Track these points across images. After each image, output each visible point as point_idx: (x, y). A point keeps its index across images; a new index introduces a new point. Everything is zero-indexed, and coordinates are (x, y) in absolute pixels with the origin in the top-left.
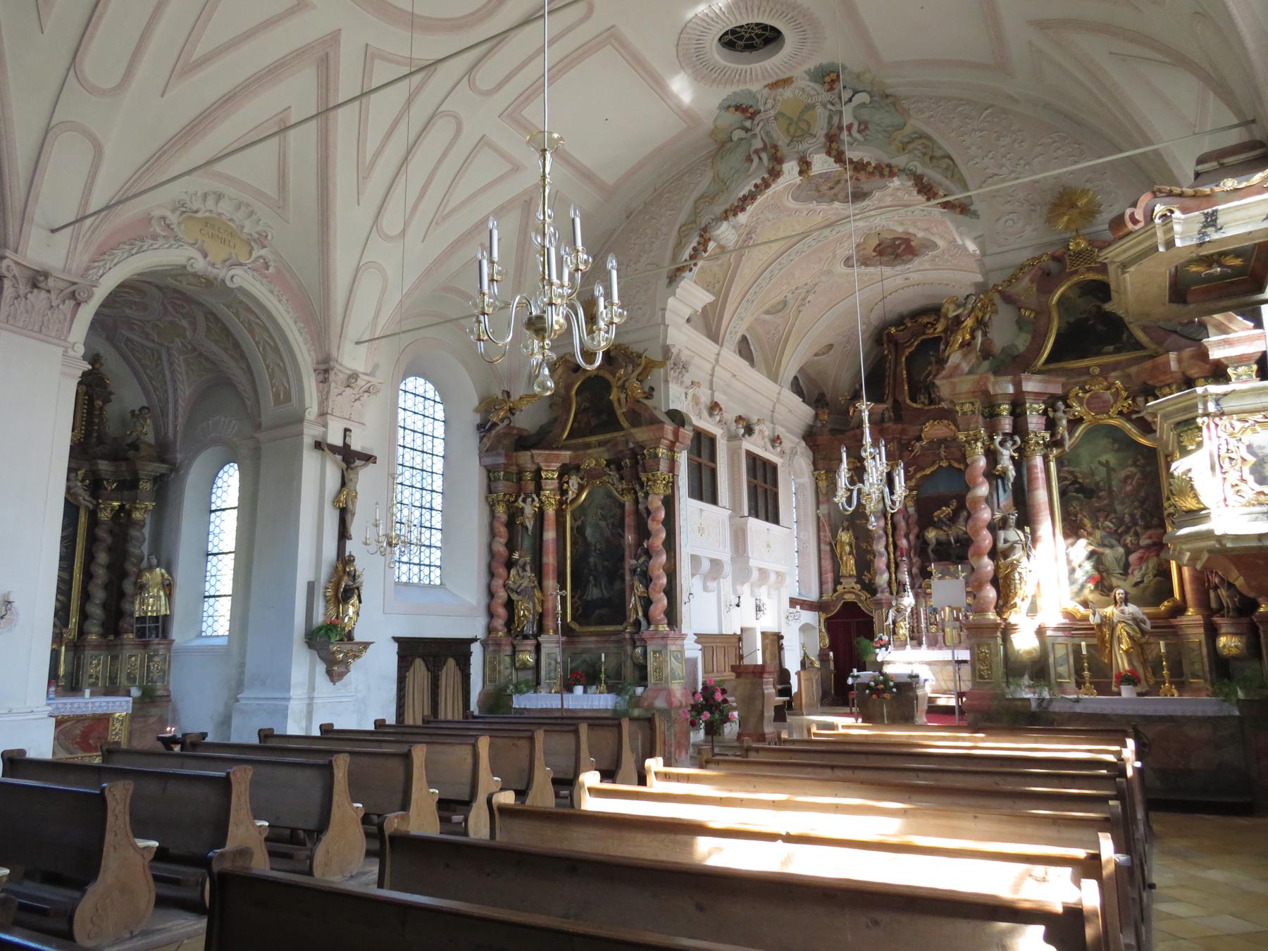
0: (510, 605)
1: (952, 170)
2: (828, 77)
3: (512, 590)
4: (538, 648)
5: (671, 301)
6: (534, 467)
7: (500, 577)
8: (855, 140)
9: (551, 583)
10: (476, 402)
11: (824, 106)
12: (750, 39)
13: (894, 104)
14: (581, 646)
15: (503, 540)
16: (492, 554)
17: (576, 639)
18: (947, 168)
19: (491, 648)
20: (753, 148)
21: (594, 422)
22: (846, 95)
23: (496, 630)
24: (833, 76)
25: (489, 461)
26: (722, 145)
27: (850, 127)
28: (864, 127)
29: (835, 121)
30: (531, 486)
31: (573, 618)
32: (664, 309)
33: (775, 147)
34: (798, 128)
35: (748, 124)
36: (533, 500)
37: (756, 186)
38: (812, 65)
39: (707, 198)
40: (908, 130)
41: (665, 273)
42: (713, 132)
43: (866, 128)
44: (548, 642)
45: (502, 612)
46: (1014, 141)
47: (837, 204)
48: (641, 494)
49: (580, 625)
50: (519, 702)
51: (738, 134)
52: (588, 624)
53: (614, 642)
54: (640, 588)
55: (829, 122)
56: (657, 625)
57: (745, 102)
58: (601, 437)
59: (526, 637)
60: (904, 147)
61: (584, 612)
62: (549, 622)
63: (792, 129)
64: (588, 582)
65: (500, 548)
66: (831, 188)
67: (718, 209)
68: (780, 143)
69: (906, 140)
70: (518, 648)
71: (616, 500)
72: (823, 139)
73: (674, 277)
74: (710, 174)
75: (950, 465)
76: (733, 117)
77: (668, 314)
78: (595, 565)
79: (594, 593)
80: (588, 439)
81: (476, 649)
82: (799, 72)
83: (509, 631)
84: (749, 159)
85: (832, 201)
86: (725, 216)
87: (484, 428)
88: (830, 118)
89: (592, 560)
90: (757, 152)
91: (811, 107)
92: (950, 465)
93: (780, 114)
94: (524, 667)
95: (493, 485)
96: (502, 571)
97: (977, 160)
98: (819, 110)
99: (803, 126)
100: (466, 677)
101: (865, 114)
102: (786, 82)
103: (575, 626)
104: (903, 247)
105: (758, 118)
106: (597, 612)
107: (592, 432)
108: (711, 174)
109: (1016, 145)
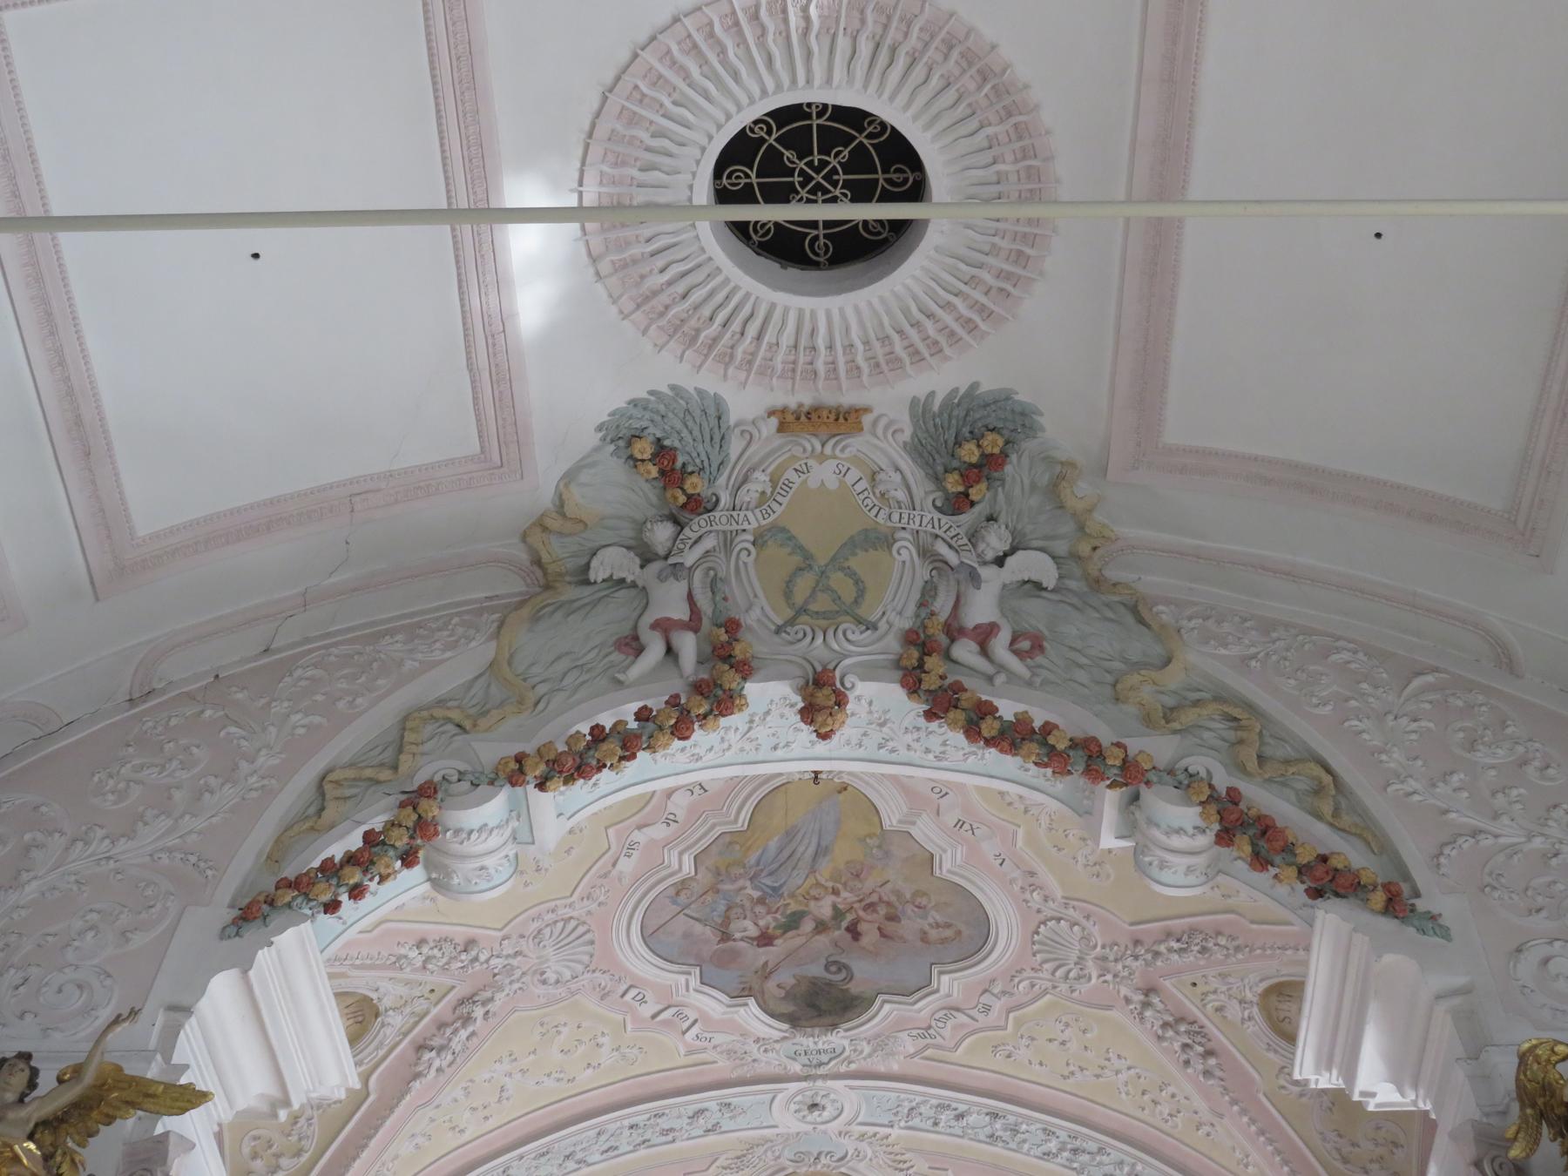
1: (1328, 791)
2: (972, 451)
5: (222, 988)
8: (1001, 668)
11: (926, 553)
12: (820, 184)
13: (1134, 610)
18: (1319, 791)
20: (648, 619)
22: (996, 541)
24: (993, 444)
26: (552, 572)
27: (984, 636)
28: (1030, 645)
29: (943, 605)
32: (181, 1010)
33: (732, 626)
34: (823, 588)
35: (662, 534)
37: (643, 715)
38: (941, 379)
39: (456, 716)
40: (1173, 679)
41: (241, 868)
42: (541, 525)
43: (1038, 646)
46: (1524, 762)
47: (751, 1016)
51: (613, 562)
55: (922, 604)
57: (688, 451)
60: (1165, 718)
63: (804, 585)
66: (765, 939)
67: (491, 750)
68: (750, 619)
69: (1170, 701)
72: (893, 644)
73: (255, 913)
74: (480, 652)
76: (620, 493)
77: (191, 1029)
82: (891, 400)
84: (633, 645)
85: (742, 992)
86: (515, 772)
88: (928, 593)
90: (665, 627)
91: (885, 541)
93: (777, 530)
97: (1412, 784)
98: (905, 551)
99: (847, 591)
101: (1036, 612)
102: (845, 420)
105: (698, 524)
108: (490, 650)
109: (1530, 770)
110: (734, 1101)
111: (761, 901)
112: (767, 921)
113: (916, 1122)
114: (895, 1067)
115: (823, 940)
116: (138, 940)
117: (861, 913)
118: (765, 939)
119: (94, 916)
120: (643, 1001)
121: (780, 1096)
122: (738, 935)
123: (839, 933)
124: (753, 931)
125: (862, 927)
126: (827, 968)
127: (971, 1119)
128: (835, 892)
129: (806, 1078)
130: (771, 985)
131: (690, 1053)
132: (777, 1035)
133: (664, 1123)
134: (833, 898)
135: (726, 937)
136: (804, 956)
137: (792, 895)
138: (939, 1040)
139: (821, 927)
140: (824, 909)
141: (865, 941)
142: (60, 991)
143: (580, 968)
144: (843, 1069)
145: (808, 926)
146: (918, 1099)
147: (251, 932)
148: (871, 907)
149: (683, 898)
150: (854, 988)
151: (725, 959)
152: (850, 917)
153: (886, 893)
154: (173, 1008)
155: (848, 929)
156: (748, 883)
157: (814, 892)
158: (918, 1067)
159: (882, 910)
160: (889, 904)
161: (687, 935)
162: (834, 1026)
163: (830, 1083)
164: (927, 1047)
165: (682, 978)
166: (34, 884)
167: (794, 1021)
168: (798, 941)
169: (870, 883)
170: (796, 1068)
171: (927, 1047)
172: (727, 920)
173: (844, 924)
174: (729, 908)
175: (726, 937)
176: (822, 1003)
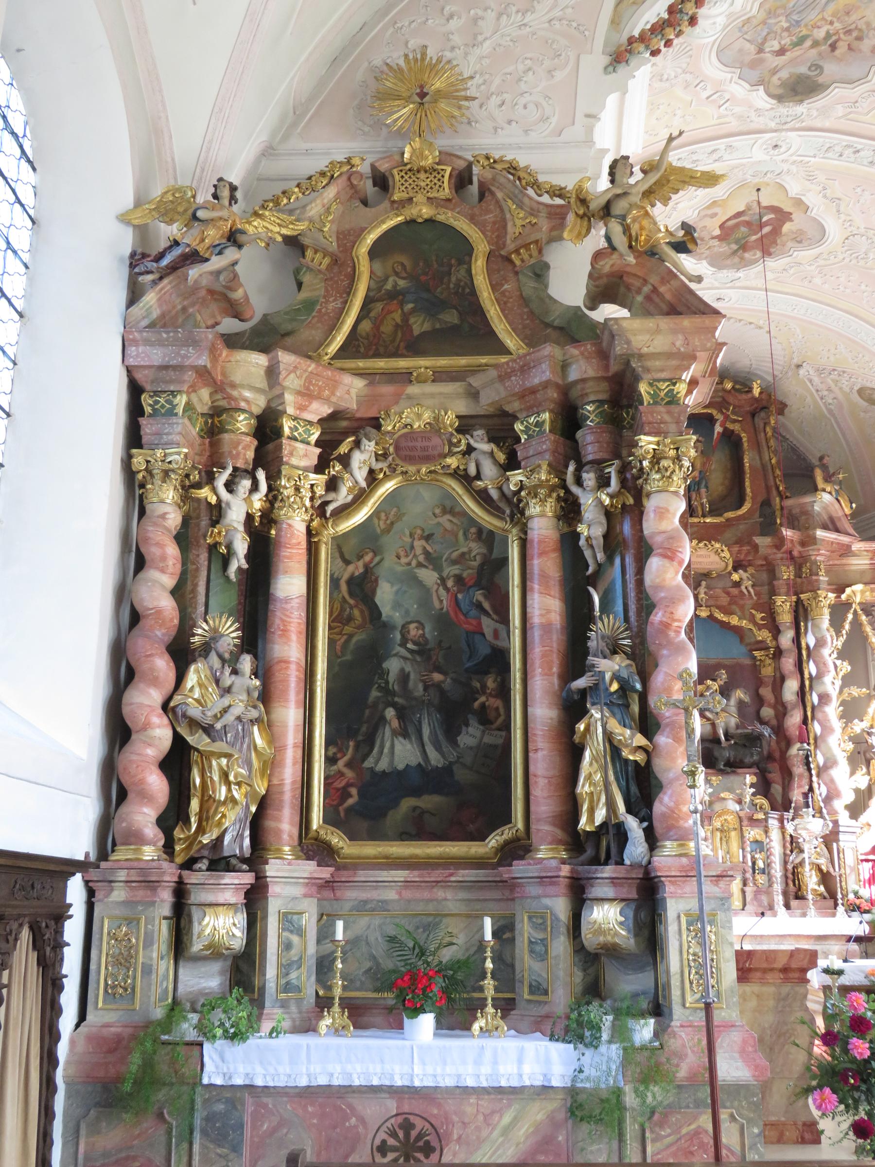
0: (177, 761)
3: (194, 724)
4: (255, 899)
6: (258, 403)
7: (155, 682)
9: (290, 715)
10: (128, 201)
14: (352, 895)
15: (169, 581)
16: (130, 617)
17: (344, 875)
19: (119, 894)
21: (419, 325)
23: (136, 838)
25: (150, 355)
30: (245, 450)
31: (330, 819)
36: (255, 487)
44: (288, 880)
45: (157, 784)
48: (592, 502)
49: (353, 837)
50: (226, 1064)
52: (375, 835)
53: (462, 885)
54: (631, 739)
56: (683, 837)
58: (443, 362)
59: (220, 863)
61: (368, 804)
62: (284, 824)
64: (382, 720)
65: (157, 593)
66: (781, 52)
70: (196, 896)
71: (472, 522)
73: (619, 57)
75: (711, 617)
78: (404, 678)
79: (399, 753)
80: (402, 363)
81: (75, 890)
83: (169, 847)
87: (147, 266)
89: (393, 666)
92: (711, 617)
94: (215, 952)
95: (148, 427)
96: (163, 666)
100: (52, 984)
103: (336, 839)
104: (766, 230)
106: (407, 804)
107: (415, 347)
110: (734, 144)
111: (787, 29)
112: (786, 41)
113: (830, 155)
114: (827, 124)
115: (814, 52)
116: (559, 75)
117: (842, 36)
118: (781, 52)
119: (528, 62)
120: (705, 89)
121: (760, 141)
122: (767, 50)
123: (825, 48)
124: (777, 47)
125: (840, 44)
126: (809, 69)
127: (862, 154)
128: (831, 23)
129: (776, 131)
130: (775, 80)
131: (719, 118)
132: (769, 106)
133: (695, 157)
134: (829, 27)
135: (761, 51)
136: (797, 63)
137: (806, 25)
138: (860, 109)
139: (816, 44)
140: (820, 34)
141: (837, 52)
142: (525, 107)
143: (680, 71)
144: (797, 126)
145: (808, 43)
146: (835, 142)
147: (622, 69)
148: (848, 32)
149: (745, 28)
150: (821, 80)
151: (754, 64)
152: (834, 38)
153: (861, 25)
154: (588, 116)
155: (830, 45)
156: (783, 18)
157: (819, 24)
158: (844, 125)
159: (855, 34)
160: (860, 30)
161: (740, 50)
162: (801, 101)
163: (789, 133)
164: (850, 113)
165: (729, 76)
166: (488, 43)
167: (780, 98)
168: (798, 53)
169: (854, 17)
170: (772, 125)
171: (850, 113)
172: (765, 40)
173: (829, 42)
174: (768, 33)
175: (761, 51)
176: (800, 89)
